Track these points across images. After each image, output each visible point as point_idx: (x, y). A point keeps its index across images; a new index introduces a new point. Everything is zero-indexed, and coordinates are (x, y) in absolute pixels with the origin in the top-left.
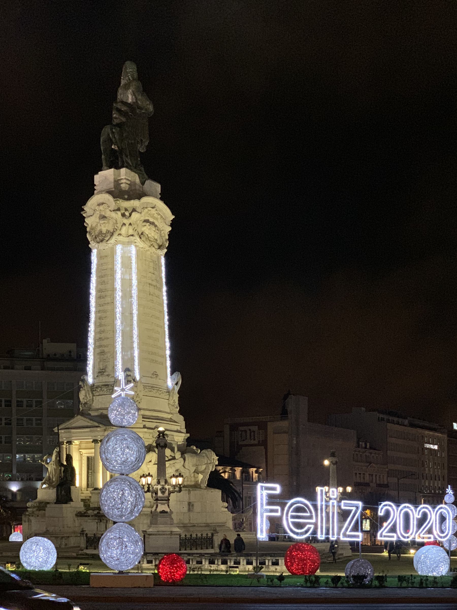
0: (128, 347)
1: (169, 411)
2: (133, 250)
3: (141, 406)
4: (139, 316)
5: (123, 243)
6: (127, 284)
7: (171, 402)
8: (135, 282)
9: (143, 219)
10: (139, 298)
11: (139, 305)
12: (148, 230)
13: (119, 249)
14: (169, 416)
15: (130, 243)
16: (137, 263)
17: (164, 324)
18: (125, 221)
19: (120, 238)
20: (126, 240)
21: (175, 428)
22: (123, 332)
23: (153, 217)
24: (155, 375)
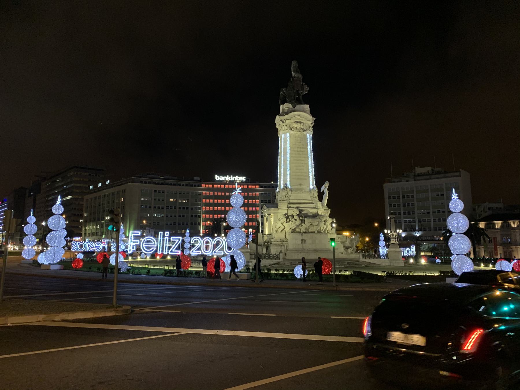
0: (285, 175)
1: (310, 199)
2: (288, 134)
3: (291, 198)
4: (290, 161)
5: (285, 133)
6: (285, 149)
7: (312, 195)
8: (288, 148)
9: (293, 121)
10: (290, 154)
11: (291, 157)
12: (295, 125)
13: (283, 135)
14: (311, 201)
15: (287, 132)
16: (290, 140)
17: (308, 162)
18: (284, 124)
19: (283, 131)
20: (285, 132)
21: (312, 206)
22: (284, 169)
23: (300, 119)
24: (300, 184)
